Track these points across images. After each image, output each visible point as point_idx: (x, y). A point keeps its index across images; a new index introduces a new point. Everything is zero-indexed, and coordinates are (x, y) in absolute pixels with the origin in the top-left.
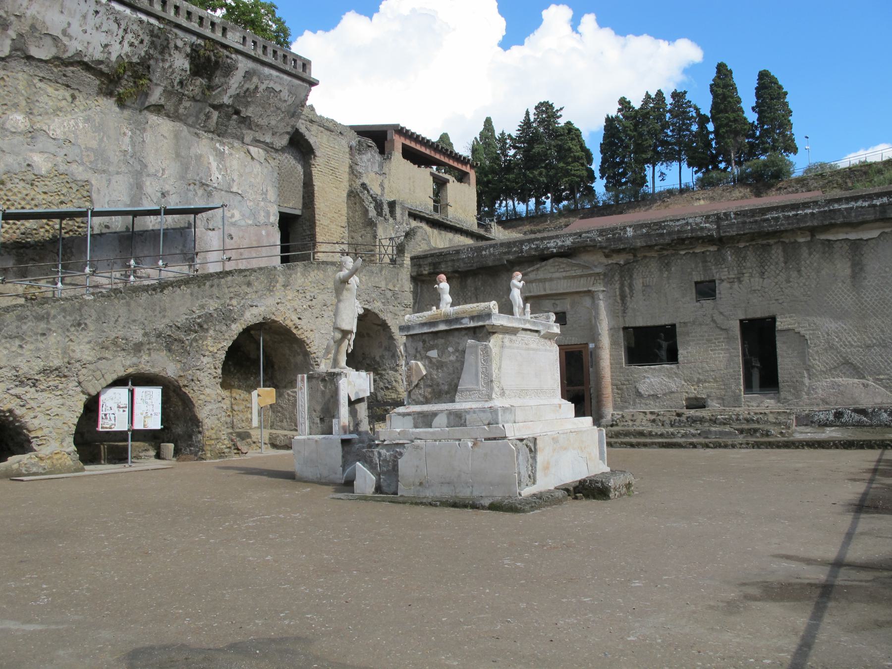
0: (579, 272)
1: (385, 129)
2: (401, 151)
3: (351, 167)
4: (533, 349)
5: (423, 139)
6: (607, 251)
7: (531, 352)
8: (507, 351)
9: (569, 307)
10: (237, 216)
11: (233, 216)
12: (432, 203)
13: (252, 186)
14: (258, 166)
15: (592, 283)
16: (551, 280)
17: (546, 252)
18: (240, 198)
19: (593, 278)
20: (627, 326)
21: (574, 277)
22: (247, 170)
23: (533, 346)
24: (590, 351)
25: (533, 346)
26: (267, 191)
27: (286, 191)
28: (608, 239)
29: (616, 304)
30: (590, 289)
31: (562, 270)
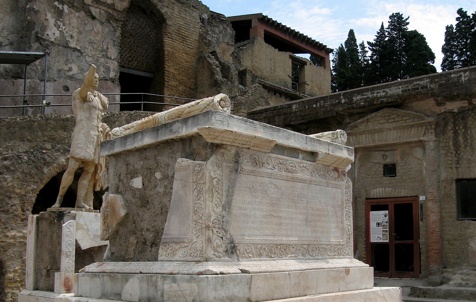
0: (410, 122)
1: (249, 18)
2: (263, 36)
3: (201, 35)
4: (302, 181)
5: (284, 27)
6: (439, 99)
7: (299, 185)
8: (243, 179)
9: (399, 158)
10: (75, 70)
11: (70, 69)
12: (291, 82)
13: (91, 43)
14: (99, 25)
15: (423, 133)
16: (381, 131)
17: (375, 103)
18: (79, 54)
19: (424, 128)
20: (461, 177)
21: (404, 128)
22: (88, 28)
23: (306, 176)
24: (420, 203)
25: (306, 176)
26: (107, 48)
27: (140, 56)
28: (441, 85)
29: (449, 154)
30: (421, 139)
31: (393, 120)
